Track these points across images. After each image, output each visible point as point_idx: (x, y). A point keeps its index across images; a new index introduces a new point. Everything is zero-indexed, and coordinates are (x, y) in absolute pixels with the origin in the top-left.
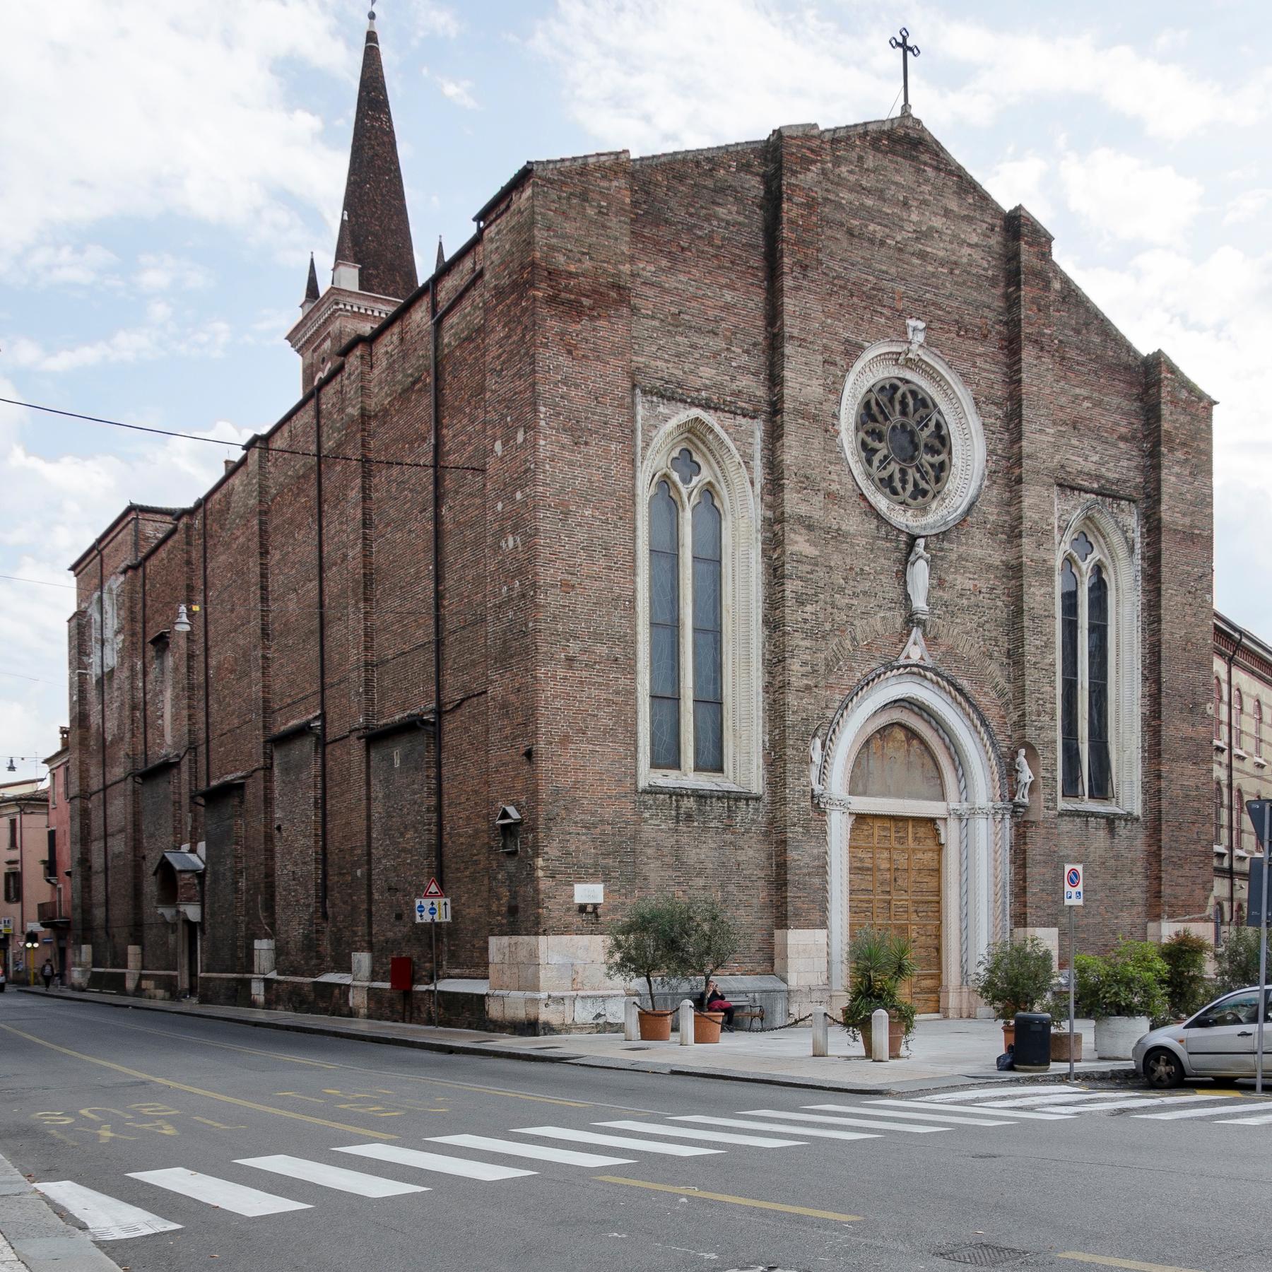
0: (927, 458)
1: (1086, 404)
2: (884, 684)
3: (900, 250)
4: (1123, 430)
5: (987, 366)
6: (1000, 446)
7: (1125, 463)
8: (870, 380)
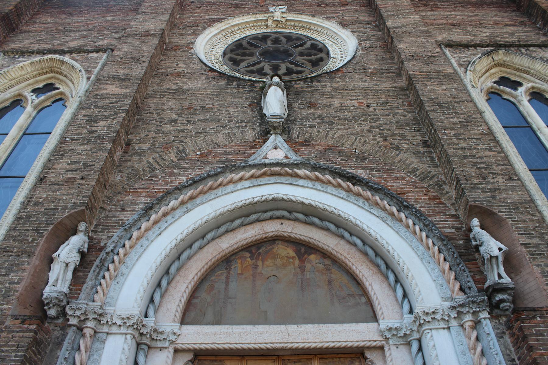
2: (231, 187)
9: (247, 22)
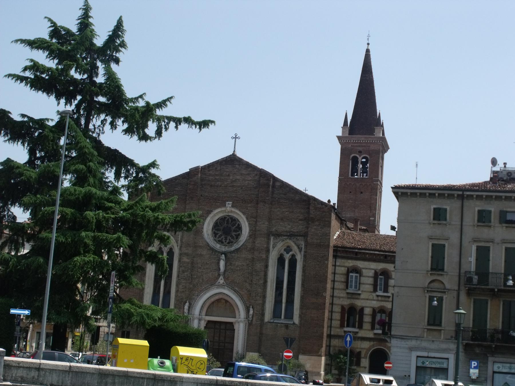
0: (233, 234)
1: (287, 213)
3: (226, 186)
4: (301, 218)
5: (252, 209)
6: (254, 228)
7: (301, 227)
8: (217, 218)
9: (220, 211)
